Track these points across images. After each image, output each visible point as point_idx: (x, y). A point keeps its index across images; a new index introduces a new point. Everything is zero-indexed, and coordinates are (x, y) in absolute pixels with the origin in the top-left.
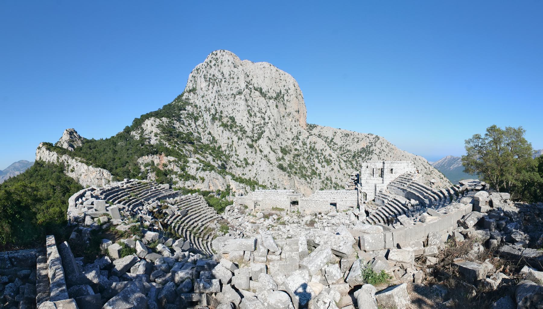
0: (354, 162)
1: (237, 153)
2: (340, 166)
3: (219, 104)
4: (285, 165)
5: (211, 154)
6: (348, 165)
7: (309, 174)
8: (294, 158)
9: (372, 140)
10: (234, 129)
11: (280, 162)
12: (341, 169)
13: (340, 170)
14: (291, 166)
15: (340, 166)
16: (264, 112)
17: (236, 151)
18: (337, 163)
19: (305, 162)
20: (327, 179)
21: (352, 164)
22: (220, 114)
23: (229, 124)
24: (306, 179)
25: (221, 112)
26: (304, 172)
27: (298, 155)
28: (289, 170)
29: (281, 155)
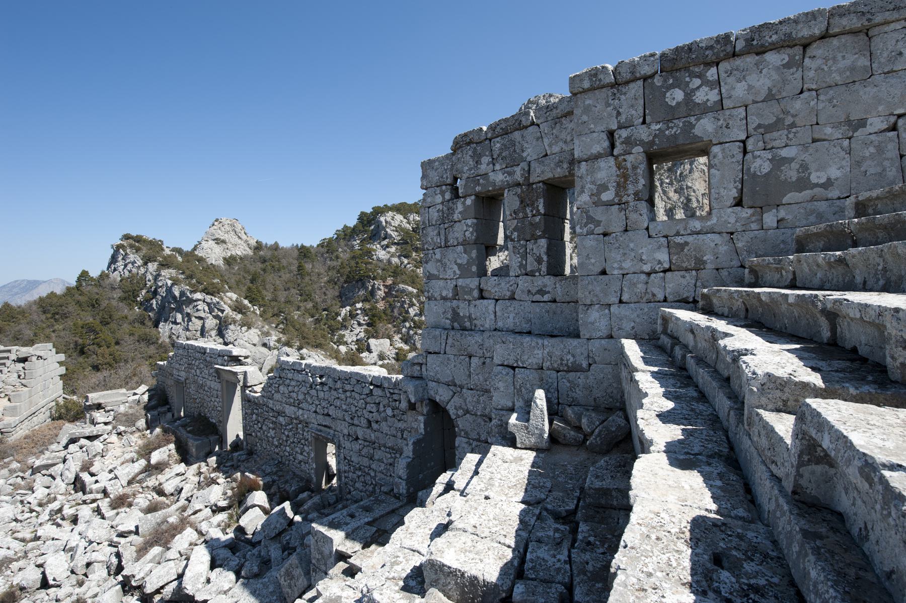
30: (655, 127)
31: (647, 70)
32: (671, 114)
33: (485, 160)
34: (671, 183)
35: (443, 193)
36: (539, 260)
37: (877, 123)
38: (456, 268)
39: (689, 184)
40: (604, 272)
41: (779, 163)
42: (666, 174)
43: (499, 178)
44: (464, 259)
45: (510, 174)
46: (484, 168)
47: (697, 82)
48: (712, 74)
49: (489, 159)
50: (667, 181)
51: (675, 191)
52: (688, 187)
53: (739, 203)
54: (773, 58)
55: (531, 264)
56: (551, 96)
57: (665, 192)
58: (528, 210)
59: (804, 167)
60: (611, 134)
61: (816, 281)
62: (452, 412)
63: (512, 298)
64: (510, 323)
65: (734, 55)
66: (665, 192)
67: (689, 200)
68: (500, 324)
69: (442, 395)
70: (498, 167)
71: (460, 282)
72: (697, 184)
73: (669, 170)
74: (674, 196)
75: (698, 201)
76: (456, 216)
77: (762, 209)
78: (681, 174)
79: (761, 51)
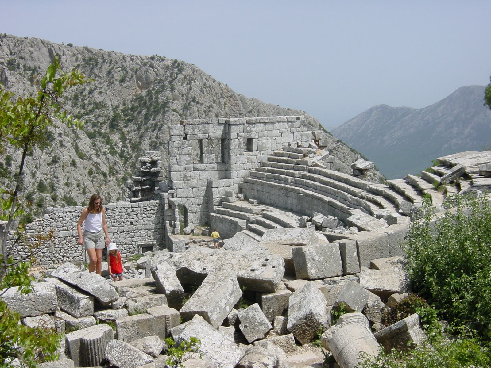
0: (115, 137)
2: (77, 149)
6: (99, 144)
9: (162, 72)
12: (82, 156)
13: (78, 160)
15: (77, 149)
18: (68, 141)
20: (41, 187)
21: (108, 142)
30: (245, 134)
31: (244, 122)
32: (248, 132)
33: (197, 130)
35: (180, 138)
36: (213, 160)
37: (274, 138)
38: (185, 161)
40: (236, 164)
41: (263, 143)
43: (201, 136)
44: (189, 159)
45: (204, 135)
46: (196, 132)
47: (252, 126)
48: (254, 125)
49: (198, 130)
53: (257, 150)
54: (262, 125)
55: (211, 160)
58: (210, 146)
59: (266, 145)
60: (237, 134)
61: (276, 167)
62: (187, 206)
63: (205, 170)
64: (205, 176)
65: (257, 123)
68: (201, 178)
69: (183, 201)
70: (200, 133)
71: (187, 166)
76: (185, 146)
77: (260, 151)
79: (261, 123)
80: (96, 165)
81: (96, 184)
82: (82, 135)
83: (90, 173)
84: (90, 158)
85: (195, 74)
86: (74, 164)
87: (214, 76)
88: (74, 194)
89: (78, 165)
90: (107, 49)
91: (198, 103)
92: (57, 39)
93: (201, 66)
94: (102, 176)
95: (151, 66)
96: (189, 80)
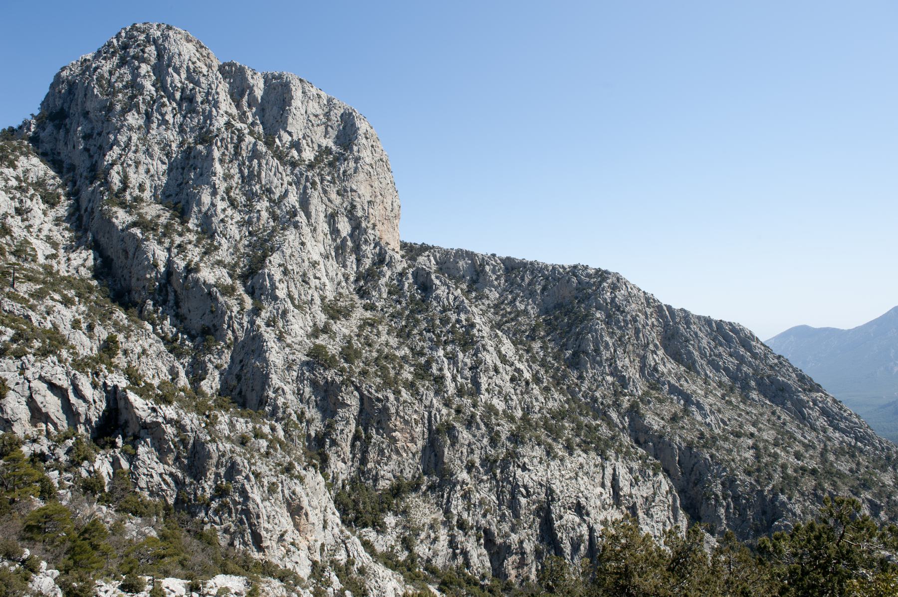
1: (183, 310)
2: (499, 352)
3: (137, 164)
4: (333, 348)
5: (67, 302)
7: (407, 374)
8: (361, 328)
10: (178, 240)
11: (318, 342)
14: (349, 353)
15: (499, 352)
16: (276, 197)
17: (177, 304)
18: (490, 344)
19: (394, 341)
22: (136, 192)
23: (163, 220)
24: (397, 393)
25: (141, 188)
26: (392, 373)
27: (372, 324)
28: (346, 365)
29: (322, 318)
34: (333, 182)
39: (354, 187)
42: (327, 170)
50: (329, 178)
51: (338, 193)
52: (352, 190)
56: (169, 28)
57: (325, 192)
66: (325, 192)
67: (353, 207)
72: (362, 187)
73: (331, 164)
74: (337, 200)
75: (363, 209)
78: (345, 172)
80: (518, 370)
81: (518, 392)
82: (505, 340)
83: (512, 380)
84: (512, 364)
85: (618, 283)
86: (496, 370)
87: (638, 285)
88: (495, 401)
89: (501, 370)
90: (529, 258)
91: (623, 311)
92: (481, 249)
93: (625, 275)
94: (524, 383)
95: (574, 275)
96: (614, 288)
